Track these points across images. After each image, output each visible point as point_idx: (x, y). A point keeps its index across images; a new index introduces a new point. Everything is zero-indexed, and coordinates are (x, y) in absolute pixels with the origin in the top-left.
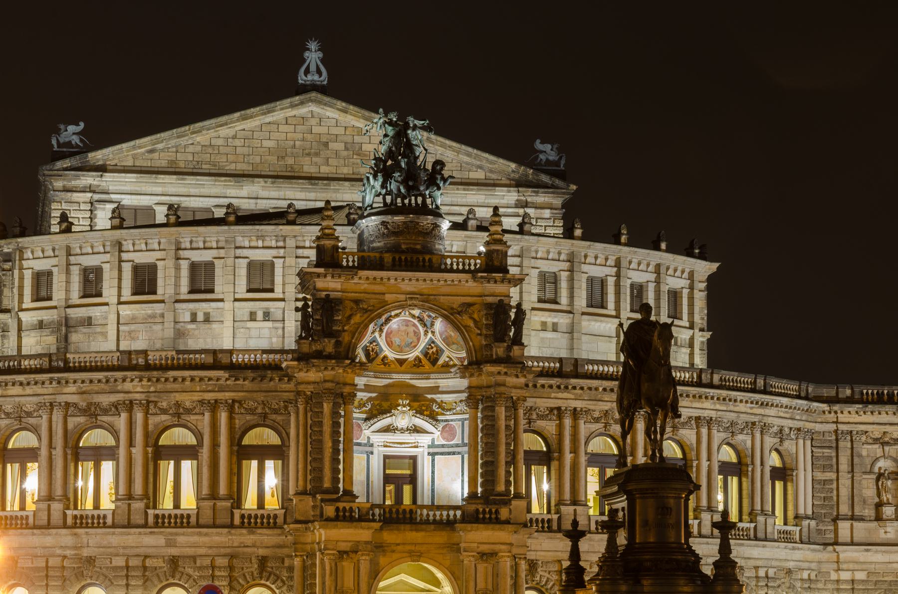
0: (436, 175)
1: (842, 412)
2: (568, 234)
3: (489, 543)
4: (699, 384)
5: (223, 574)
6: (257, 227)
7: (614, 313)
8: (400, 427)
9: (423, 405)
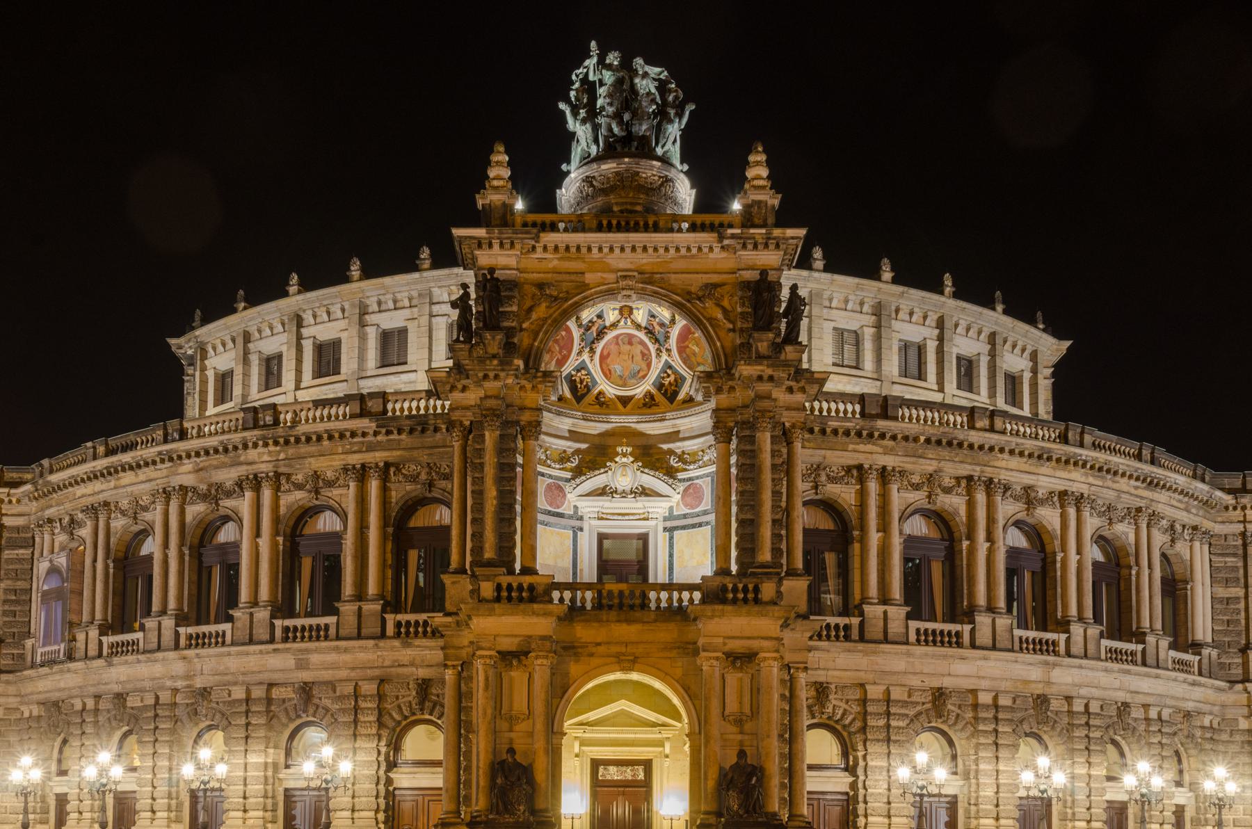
8: (620, 489)
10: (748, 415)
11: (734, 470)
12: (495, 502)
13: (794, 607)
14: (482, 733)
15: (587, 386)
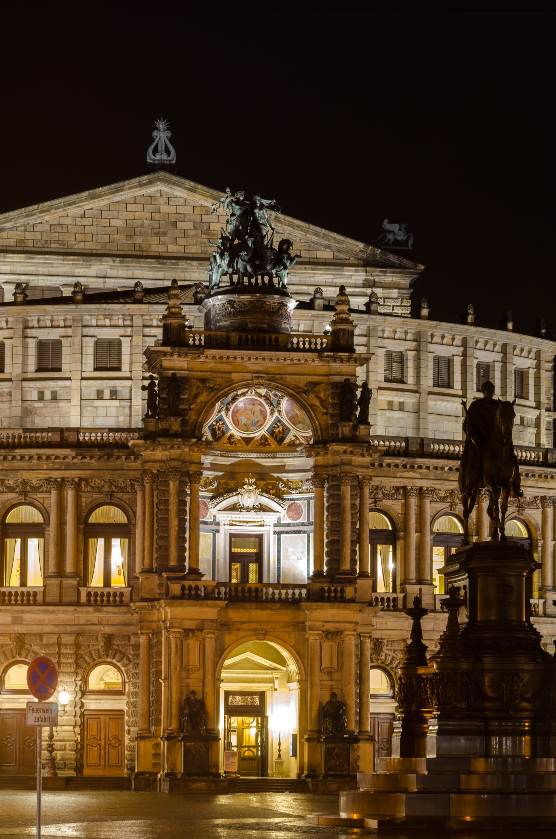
0: (283, 255)
2: (415, 314)
3: (334, 622)
4: (545, 464)
5: (69, 651)
6: (105, 306)
7: (460, 393)
8: (246, 505)
12: (177, 529)
15: (222, 432)
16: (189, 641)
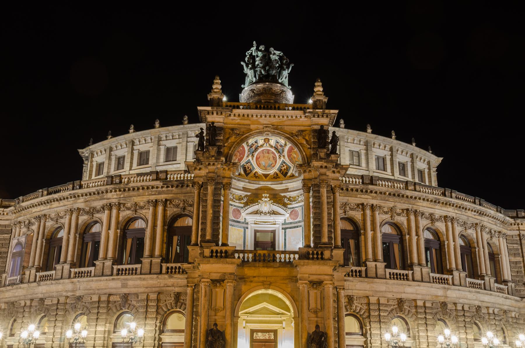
1: (522, 224)
3: (316, 275)
5: (153, 304)
8: (264, 211)
9: (277, 198)
10: (317, 181)
11: (311, 204)
12: (211, 215)
13: (338, 261)
14: (203, 316)
15: (250, 170)
16: (217, 290)
